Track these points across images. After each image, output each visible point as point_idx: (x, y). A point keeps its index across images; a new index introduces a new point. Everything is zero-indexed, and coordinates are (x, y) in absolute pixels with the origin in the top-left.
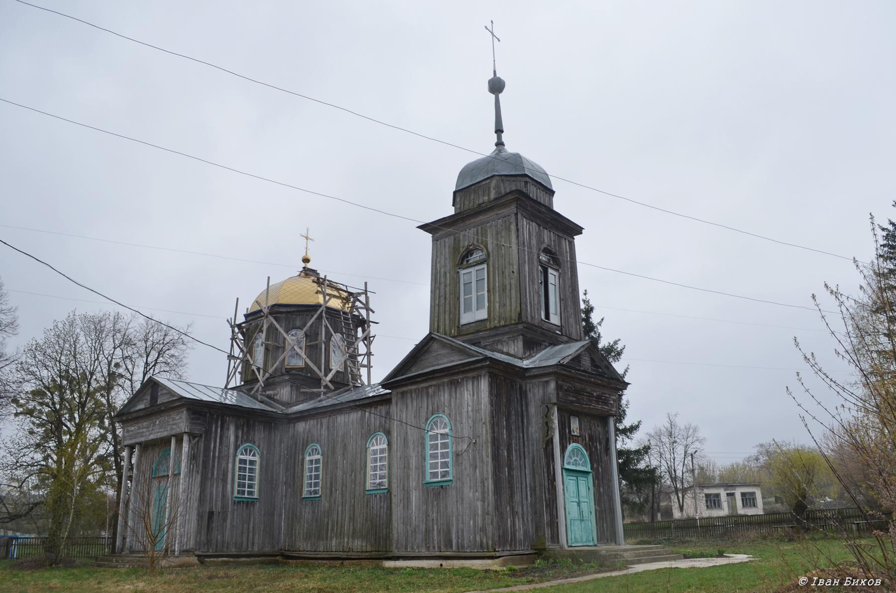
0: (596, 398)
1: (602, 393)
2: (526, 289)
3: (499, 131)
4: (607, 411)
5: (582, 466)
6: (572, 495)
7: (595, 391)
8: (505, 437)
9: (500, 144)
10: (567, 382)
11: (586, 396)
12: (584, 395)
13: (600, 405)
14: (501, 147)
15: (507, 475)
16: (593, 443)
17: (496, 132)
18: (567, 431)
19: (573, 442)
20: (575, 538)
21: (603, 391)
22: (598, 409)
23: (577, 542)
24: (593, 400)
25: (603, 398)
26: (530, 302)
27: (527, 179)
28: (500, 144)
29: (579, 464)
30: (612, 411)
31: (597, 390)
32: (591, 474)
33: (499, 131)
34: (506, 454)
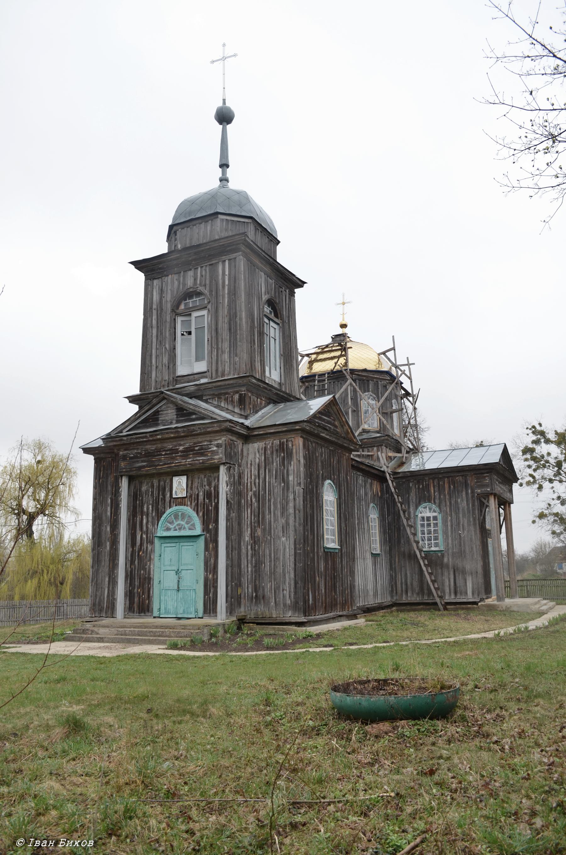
0: (182, 452)
1: (195, 443)
2: (151, 356)
3: (224, 165)
4: (203, 463)
5: (190, 529)
6: (167, 562)
7: (181, 445)
8: (109, 514)
9: (224, 180)
10: (134, 449)
11: (166, 454)
12: (162, 455)
13: (190, 458)
14: (225, 182)
15: (108, 548)
16: (210, 501)
17: (221, 166)
18: (168, 495)
19: (176, 506)
20: (165, 609)
21: (195, 441)
22: (186, 465)
23: (165, 613)
24: (176, 456)
25: (197, 448)
26: (157, 367)
27: (175, 228)
28: (224, 180)
29: (184, 528)
30: (214, 459)
31: (182, 443)
32: (203, 538)
33: (224, 165)
34: (108, 529)
